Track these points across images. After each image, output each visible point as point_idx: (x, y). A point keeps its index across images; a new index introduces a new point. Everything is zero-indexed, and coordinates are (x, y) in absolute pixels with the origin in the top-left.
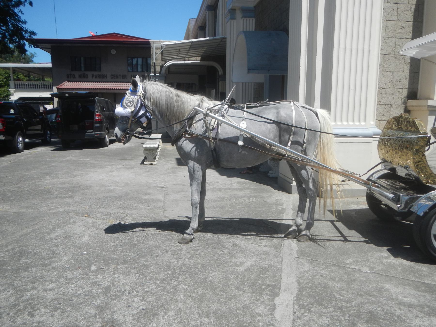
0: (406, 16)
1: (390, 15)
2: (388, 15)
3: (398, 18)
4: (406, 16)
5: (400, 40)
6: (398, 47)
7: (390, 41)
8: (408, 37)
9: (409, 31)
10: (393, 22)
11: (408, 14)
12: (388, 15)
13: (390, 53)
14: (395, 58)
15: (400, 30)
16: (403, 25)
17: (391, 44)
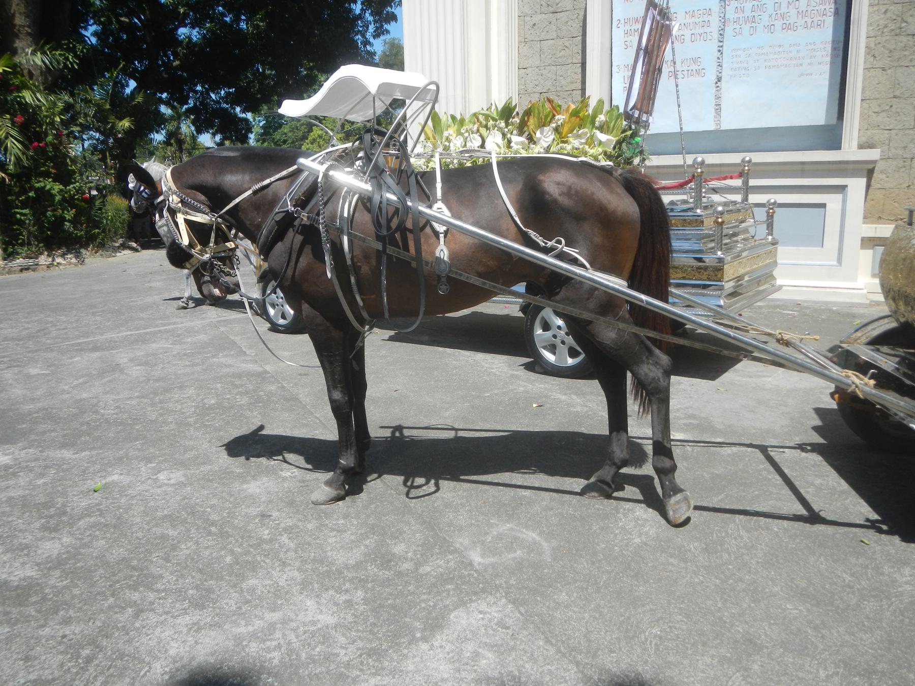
0: (571, 29)
1: (545, 33)
2: (543, 31)
3: (559, 34)
4: (571, 29)
5: (563, 68)
6: (561, 78)
7: (547, 72)
8: (575, 61)
9: (576, 51)
10: (550, 42)
11: (574, 26)
12: (543, 31)
13: (549, 89)
14: (559, 96)
15: (563, 53)
16: (567, 44)
17: (549, 75)
